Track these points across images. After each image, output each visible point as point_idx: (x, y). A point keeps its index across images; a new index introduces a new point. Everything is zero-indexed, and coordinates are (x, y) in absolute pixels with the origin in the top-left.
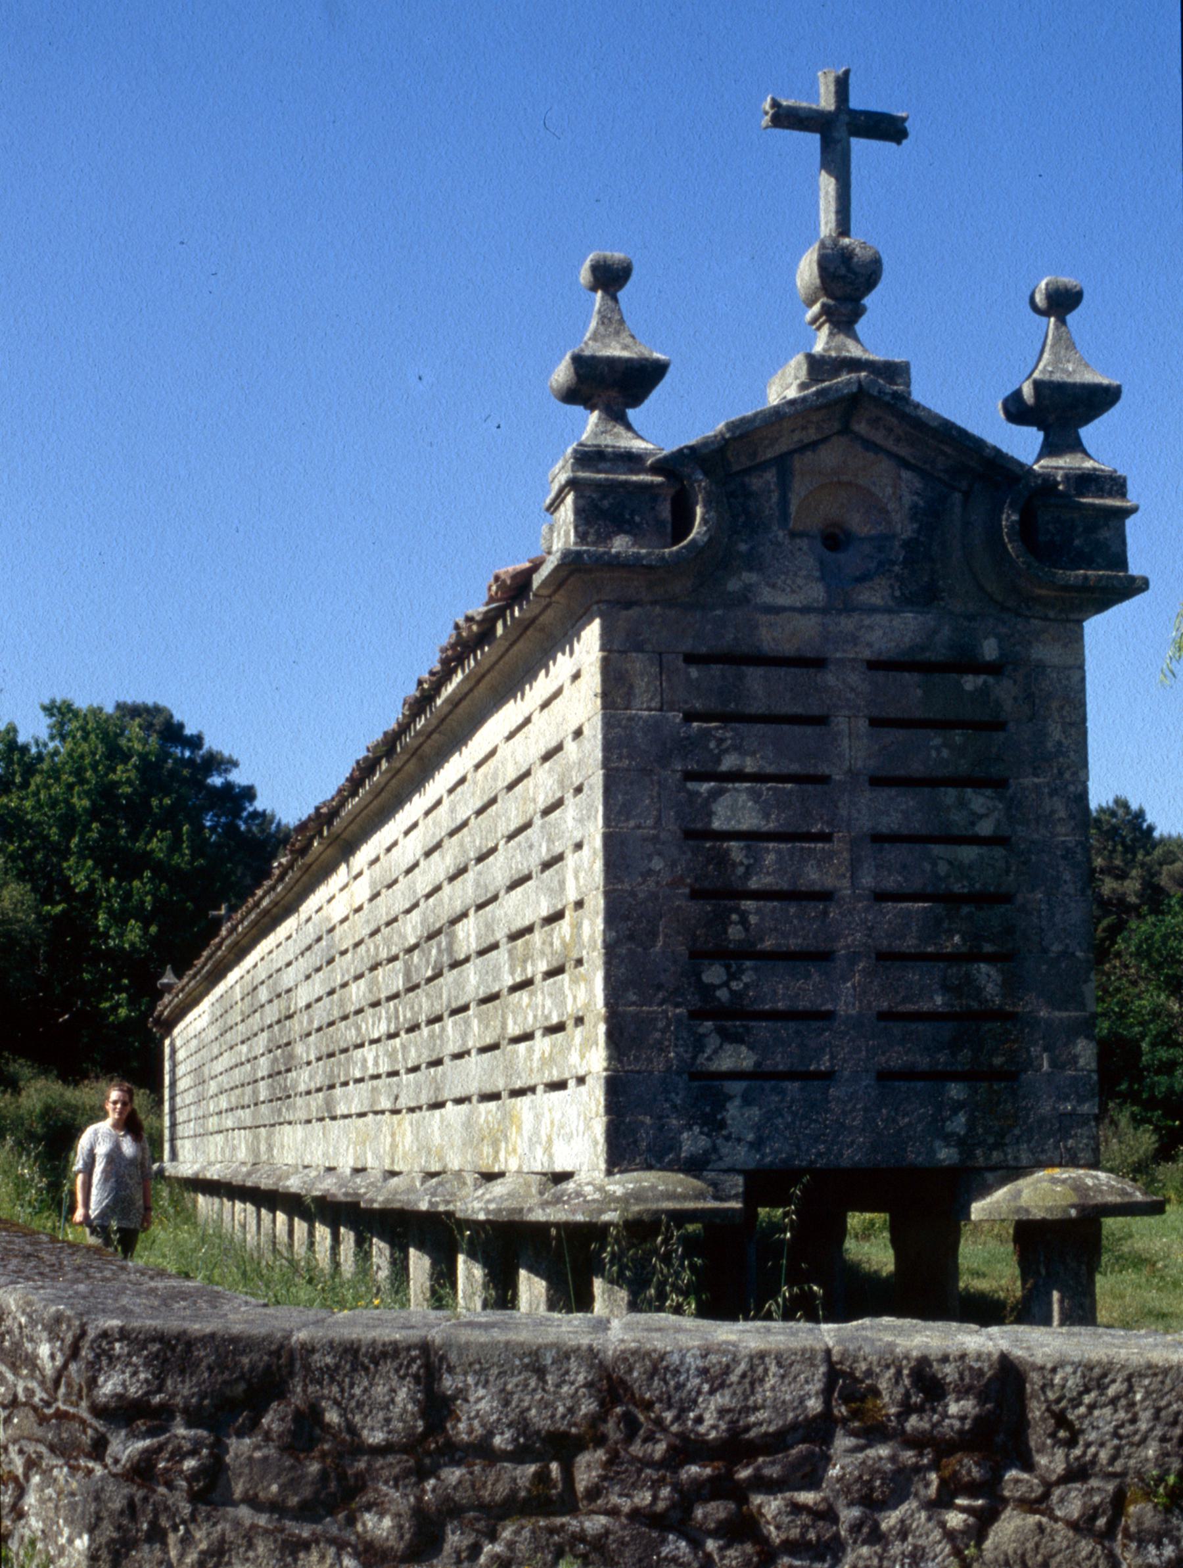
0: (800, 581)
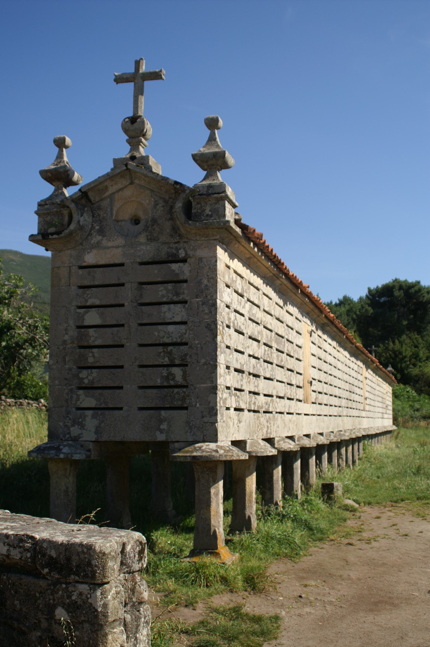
0: (115, 237)
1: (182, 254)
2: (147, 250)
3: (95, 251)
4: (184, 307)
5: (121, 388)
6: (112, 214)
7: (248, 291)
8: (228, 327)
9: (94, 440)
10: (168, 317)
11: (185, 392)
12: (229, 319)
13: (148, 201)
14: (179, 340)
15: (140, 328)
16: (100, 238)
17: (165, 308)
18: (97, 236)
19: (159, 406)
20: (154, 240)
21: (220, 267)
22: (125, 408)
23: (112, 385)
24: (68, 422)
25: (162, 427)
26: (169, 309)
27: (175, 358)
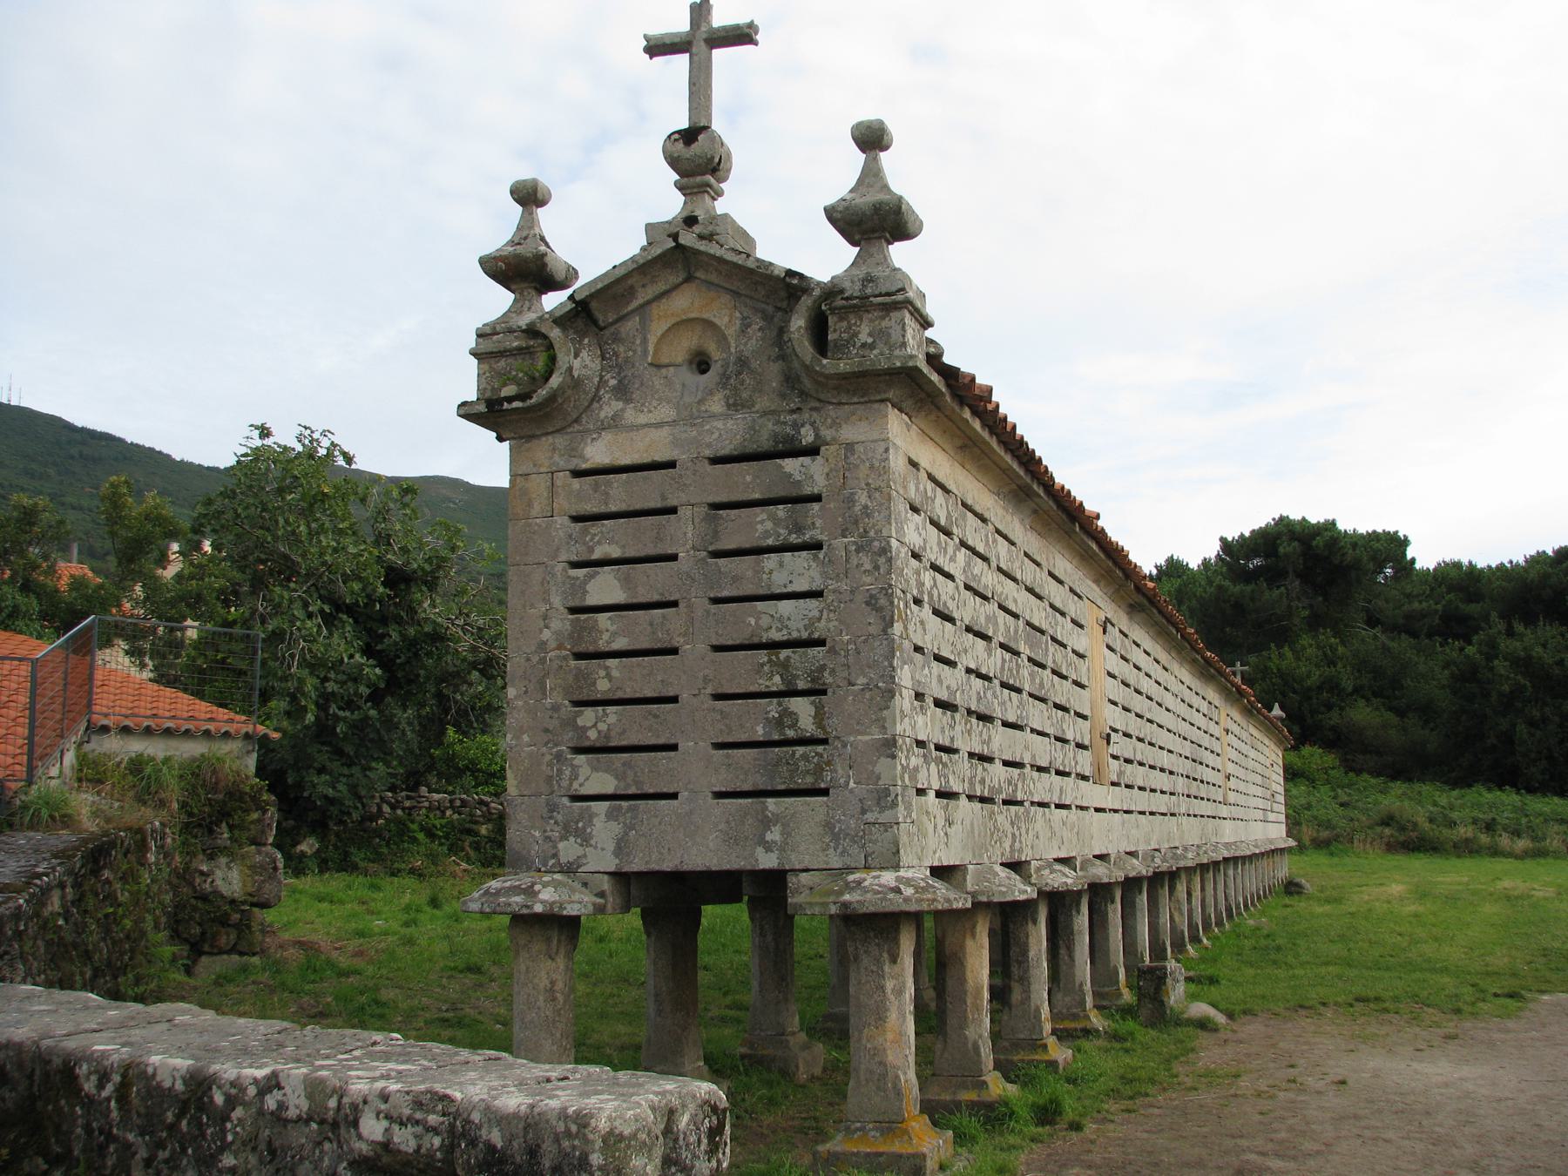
0: (655, 403)
1: (807, 437)
2: (727, 432)
3: (607, 436)
4: (815, 558)
5: (674, 747)
6: (645, 352)
7: (960, 522)
8: (918, 602)
9: (612, 869)
10: (779, 582)
11: (821, 756)
12: (921, 584)
13: (726, 319)
14: (805, 635)
15: (714, 608)
16: (620, 405)
17: (770, 561)
18: (613, 403)
19: (761, 787)
20: (743, 406)
21: (897, 463)
22: (683, 795)
23: (653, 741)
25: (769, 837)
26: (781, 565)
27: (796, 677)
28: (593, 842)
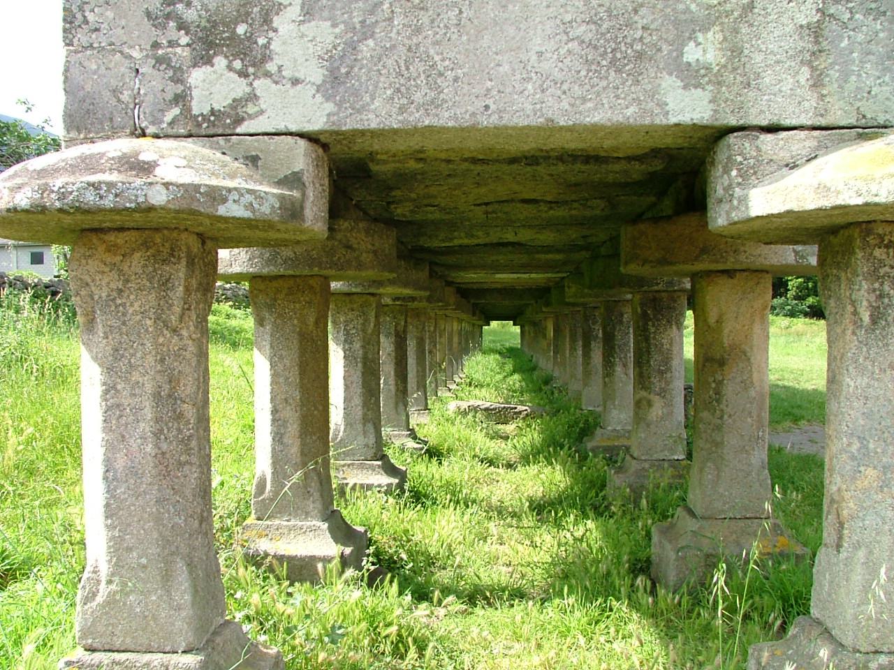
9: (317, 123)
24: (171, 44)
25: (692, 54)
28: (271, 67)
